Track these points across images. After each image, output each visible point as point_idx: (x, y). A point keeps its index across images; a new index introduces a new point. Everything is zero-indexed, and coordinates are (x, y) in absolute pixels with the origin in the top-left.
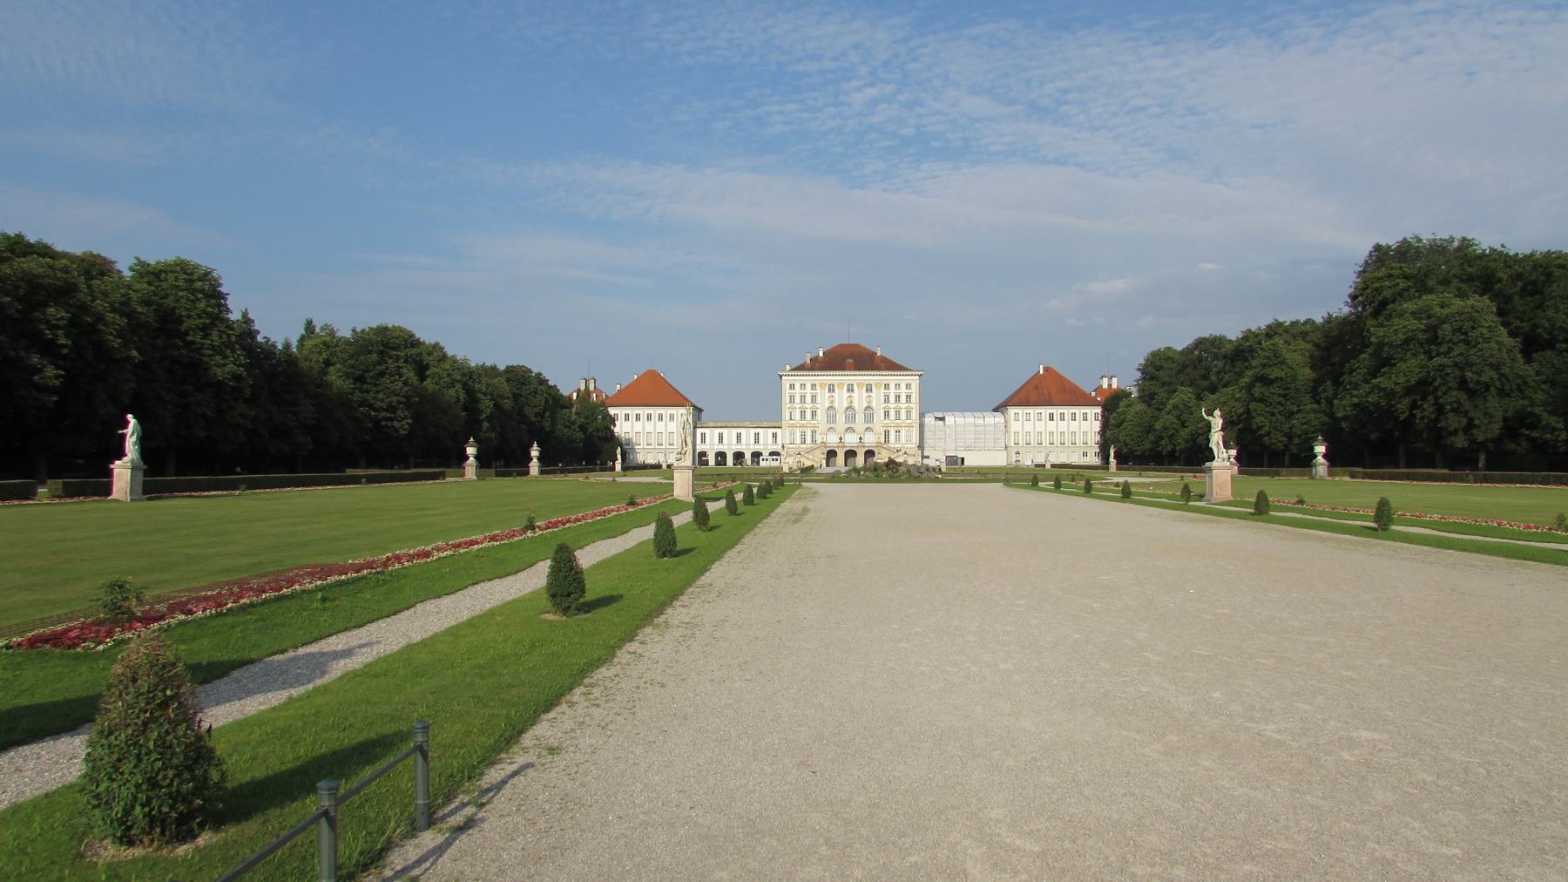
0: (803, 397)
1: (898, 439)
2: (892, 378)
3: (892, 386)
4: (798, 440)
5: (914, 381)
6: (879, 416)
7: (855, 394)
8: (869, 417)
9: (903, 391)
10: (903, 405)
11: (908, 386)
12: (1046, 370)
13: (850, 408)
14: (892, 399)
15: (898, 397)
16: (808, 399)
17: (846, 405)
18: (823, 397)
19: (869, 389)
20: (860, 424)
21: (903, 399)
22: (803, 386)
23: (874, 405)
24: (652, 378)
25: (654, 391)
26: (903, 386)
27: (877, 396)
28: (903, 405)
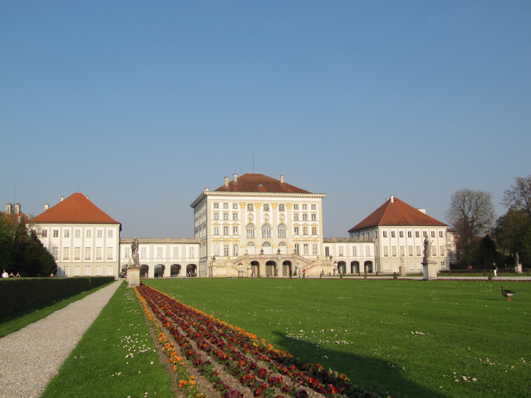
0: (226, 214)
1: (306, 252)
3: (300, 206)
4: (222, 253)
5: (318, 201)
6: (290, 232)
7: (270, 213)
9: (309, 211)
11: (313, 207)
12: (395, 200)
13: (266, 225)
14: (301, 217)
15: (305, 216)
16: (231, 217)
17: (262, 222)
19: (282, 208)
20: (275, 239)
21: (309, 217)
22: (226, 205)
23: (286, 222)
24: (78, 199)
25: (79, 211)
26: (309, 206)
27: (289, 213)
28: (310, 223)
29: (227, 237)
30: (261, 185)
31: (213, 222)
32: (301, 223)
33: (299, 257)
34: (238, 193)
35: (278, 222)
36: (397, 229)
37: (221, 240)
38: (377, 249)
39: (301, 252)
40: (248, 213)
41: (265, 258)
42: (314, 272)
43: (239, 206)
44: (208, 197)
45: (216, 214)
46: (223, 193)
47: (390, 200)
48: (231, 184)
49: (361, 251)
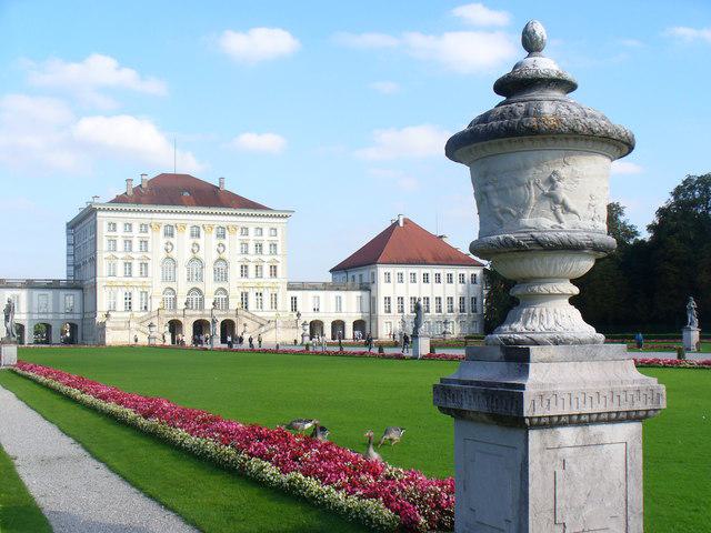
0: (128, 242)
2: (251, 222)
4: (121, 306)
6: (234, 271)
7: (200, 241)
8: (221, 275)
9: (266, 238)
10: (267, 257)
12: (405, 223)
14: (252, 249)
15: (259, 247)
16: (136, 246)
18: (158, 241)
21: (266, 248)
22: (129, 226)
23: (225, 255)
27: (233, 242)
28: (267, 257)
29: (130, 279)
30: (186, 194)
31: (105, 255)
32: (253, 257)
33: (246, 314)
34: (150, 208)
35: (215, 256)
36: (406, 270)
37: (119, 284)
38: (373, 302)
39: (252, 306)
40: (165, 240)
41: (191, 316)
42: (271, 338)
43: (150, 229)
44: (99, 214)
45: (113, 241)
46: (124, 207)
47: (397, 222)
48: (137, 190)
49: (347, 306)
